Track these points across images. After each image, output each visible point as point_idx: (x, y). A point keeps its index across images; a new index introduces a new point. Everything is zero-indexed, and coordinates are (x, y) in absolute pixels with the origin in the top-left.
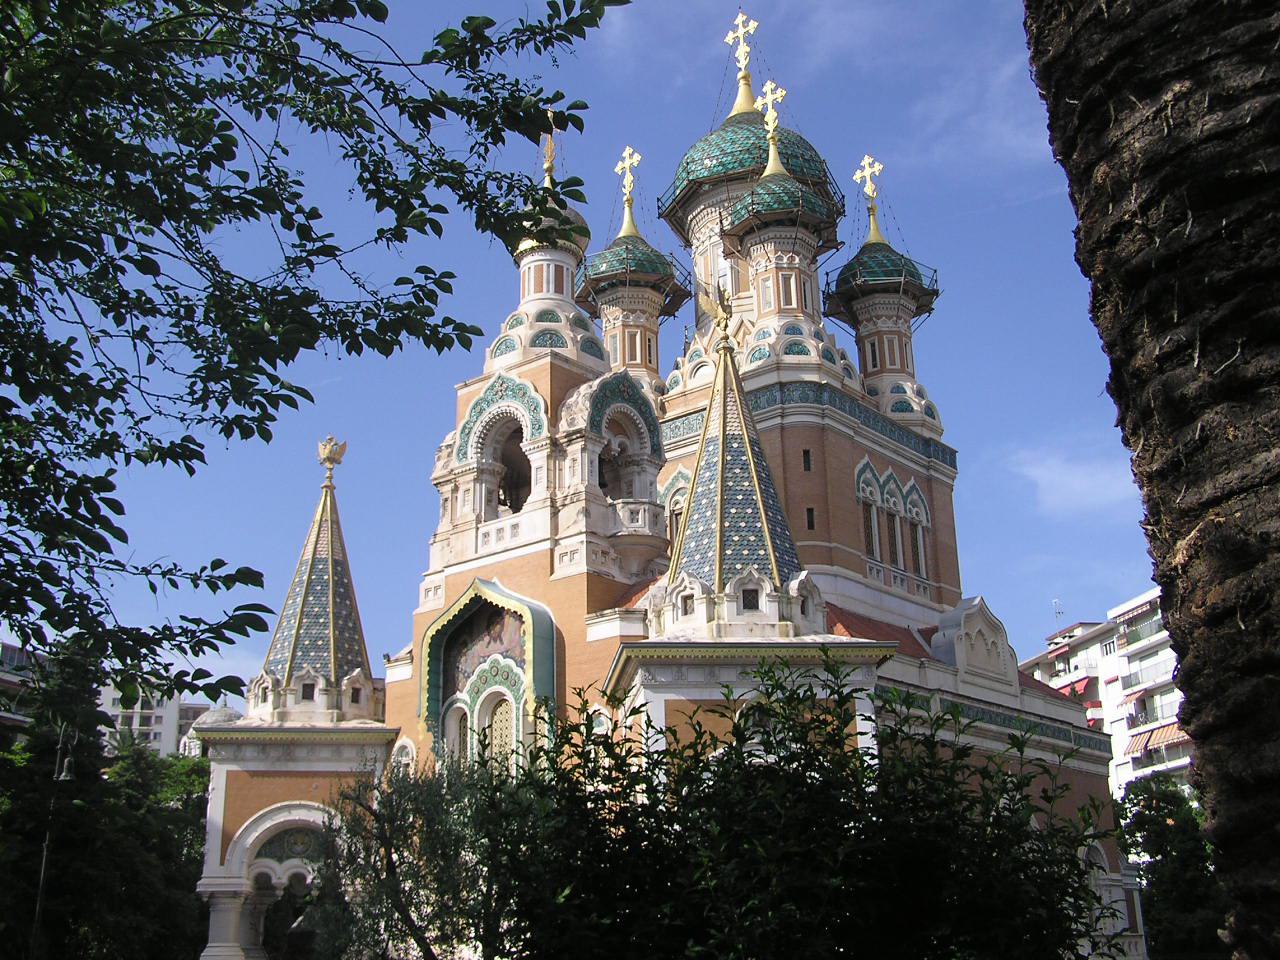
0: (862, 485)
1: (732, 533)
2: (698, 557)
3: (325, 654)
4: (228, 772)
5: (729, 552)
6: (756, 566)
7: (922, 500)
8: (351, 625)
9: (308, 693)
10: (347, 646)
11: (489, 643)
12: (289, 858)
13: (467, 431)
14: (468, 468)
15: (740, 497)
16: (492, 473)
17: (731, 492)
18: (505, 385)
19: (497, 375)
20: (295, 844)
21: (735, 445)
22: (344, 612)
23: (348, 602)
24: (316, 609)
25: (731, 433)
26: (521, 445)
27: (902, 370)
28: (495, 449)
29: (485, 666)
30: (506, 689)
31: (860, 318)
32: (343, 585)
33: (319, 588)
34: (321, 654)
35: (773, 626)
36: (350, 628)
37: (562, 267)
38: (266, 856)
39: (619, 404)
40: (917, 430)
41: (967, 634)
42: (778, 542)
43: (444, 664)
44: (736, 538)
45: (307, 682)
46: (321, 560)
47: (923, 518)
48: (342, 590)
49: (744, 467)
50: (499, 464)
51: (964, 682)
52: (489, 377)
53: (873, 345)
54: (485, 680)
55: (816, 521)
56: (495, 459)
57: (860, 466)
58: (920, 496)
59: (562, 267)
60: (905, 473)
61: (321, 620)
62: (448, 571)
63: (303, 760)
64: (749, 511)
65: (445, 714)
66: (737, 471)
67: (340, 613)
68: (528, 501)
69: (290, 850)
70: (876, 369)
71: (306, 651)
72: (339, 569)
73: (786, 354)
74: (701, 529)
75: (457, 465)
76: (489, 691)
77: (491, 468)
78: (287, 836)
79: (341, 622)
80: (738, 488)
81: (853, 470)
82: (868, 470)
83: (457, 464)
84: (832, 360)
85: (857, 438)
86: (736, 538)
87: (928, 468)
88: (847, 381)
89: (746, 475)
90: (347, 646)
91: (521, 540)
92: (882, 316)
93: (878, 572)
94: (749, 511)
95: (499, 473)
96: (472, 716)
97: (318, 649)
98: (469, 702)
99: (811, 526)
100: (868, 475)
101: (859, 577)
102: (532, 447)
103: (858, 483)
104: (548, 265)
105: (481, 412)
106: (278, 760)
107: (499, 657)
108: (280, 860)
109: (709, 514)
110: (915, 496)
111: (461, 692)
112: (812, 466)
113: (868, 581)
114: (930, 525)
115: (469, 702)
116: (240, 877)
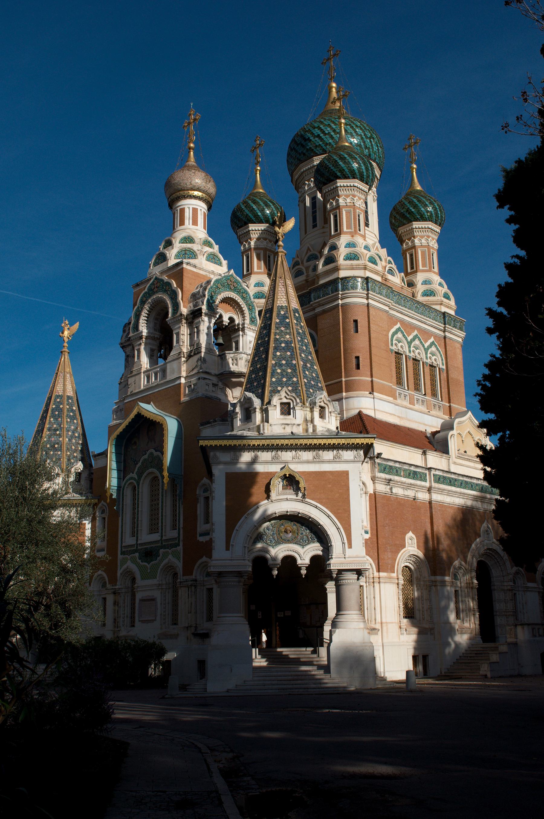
0: (394, 342)
1: (277, 368)
2: (255, 384)
3: (59, 453)
5: (274, 380)
6: (290, 388)
7: (440, 352)
8: (77, 435)
10: (73, 447)
13: (138, 313)
14: (138, 336)
15: (283, 345)
17: (278, 342)
18: (159, 284)
19: (154, 277)
21: (282, 313)
22: (73, 427)
23: (75, 421)
24: (55, 426)
25: (280, 305)
26: (167, 320)
27: (430, 271)
28: (155, 323)
29: (146, 457)
30: (156, 471)
31: (404, 239)
32: (72, 411)
33: (57, 413)
34: (56, 453)
35: (299, 425)
36: (76, 437)
37: (197, 209)
39: (227, 293)
40: (437, 307)
41: (459, 434)
42: (307, 373)
43: (124, 457)
44: (279, 371)
46: (58, 396)
47: (439, 362)
48: (71, 414)
49: (287, 326)
50: (158, 333)
51: (455, 463)
52: (150, 279)
53: (411, 255)
55: (361, 364)
56: (155, 330)
57: (393, 330)
58: (437, 349)
59: (197, 209)
60: (427, 334)
61: (58, 432)
64: (289, 353)
65: (124, 487)
66: (283, 329)
67: (70, 428)
68: (171, 354)
70: (413, 270)
72: (70, 401)
73: (345, 260)
74: (258, 366)
77: (151, 335)
79: (70, 433)
80: (282, 339)
81: (389, 331)
82: (400, 332)
84: (375, 263)
85: (392, 312)
86: (279, 371)
87: (444, 331)
88: (390, 277)
89: (288, 331)
90: (73, 447)
92: (417, 237)
93: (405, 395)
94: (289, 353)
95: (157, 339)
96: (138, 488)
97: (56, 450)
98: (137, 478)
99: (358, 367)
100: (399, 335)
101: (391, 399)
102: (173, 321)
103: (392, 340)
104: (189, 208)
107: (153, 451)
109: (263, 356)
110: (433, 349)
111: (133, 473)
112: (359, 330)
113: (399, 401)
114: (444, 367)
115: (137, 478)
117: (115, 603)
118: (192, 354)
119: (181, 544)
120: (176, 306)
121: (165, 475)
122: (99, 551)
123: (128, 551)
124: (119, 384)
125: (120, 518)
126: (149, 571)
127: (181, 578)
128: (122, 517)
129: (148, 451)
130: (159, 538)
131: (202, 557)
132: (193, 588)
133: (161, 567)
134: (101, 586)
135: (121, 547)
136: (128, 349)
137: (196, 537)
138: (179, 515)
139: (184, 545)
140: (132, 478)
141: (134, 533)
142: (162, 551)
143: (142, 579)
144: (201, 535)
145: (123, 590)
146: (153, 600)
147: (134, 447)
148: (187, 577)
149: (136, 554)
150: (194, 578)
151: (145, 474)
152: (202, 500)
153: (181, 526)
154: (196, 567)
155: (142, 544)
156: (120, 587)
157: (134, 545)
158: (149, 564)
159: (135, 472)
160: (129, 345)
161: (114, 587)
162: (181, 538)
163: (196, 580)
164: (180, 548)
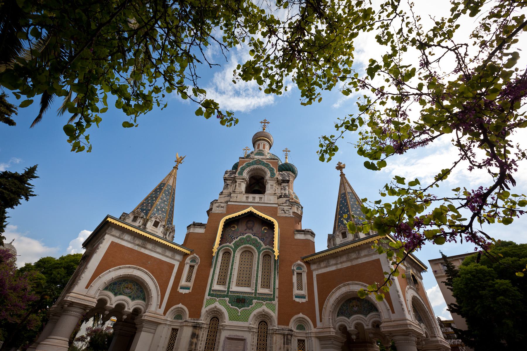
4: (112, 242)
9: (156, 224)
11: (246, 230)
12: (121, 294)
16: (247, 183)
20: (127, 288)
29: (245, 236)
38: (110, 290)
45: (158, 220)
52: (253, 159)
54: (242, 242)
62: (229, 203)
63: (149, 249)
69: (123, 290)
71: (158, 210)
75: (238, 176)
76: (248, 245)
78: (124, 283)
83: (238, 176)
91: (263, 201)
96: (234, 253)
97: (162, 211)
105: (248, 166)
106: (138, 245)
108: (116, 295)
111: (230, 243)
116: (94, 298)
117: (194, 335)
118: (283, 197)
119: (276, 300)
120: (273, 175)
121: (275, 250)
122: (181, 288)
123: (215, 294)
124: (220, 195)
125: (212, 270)
126: (239, 314)
127: (275, 325)
128: (215, 269)
129: (245, 234)
130: (253, 291)
131: (299, 313)
132: (289, 337)
133: (255, 312)
134: (173, 318)
135: (210, 289)
136: (229, 182)
137: (292, 297)
138: (275, 279)
139: (279, 301)
140: (228, 246)
141: (221, 282)
142: (254, 301)
143: (230, 319)
144: (296, 297)
145: (205, 326)
146: (244, 340)
147: (234, 229)
148: (283, 327)
149: (226, 298)
150: (290, 328)
151: (242, 246)
152: (295, 273)
153: (277, 286)
154: (292, 320)
155: (234, 292)
156: (203, 322)
157: (225, 291)
158: (240, 309)
159: (232, 244)
160: (231, 180)
161: (196, 322)
162: (277, 294)
163: (292, 331)
164: (276, 302)
